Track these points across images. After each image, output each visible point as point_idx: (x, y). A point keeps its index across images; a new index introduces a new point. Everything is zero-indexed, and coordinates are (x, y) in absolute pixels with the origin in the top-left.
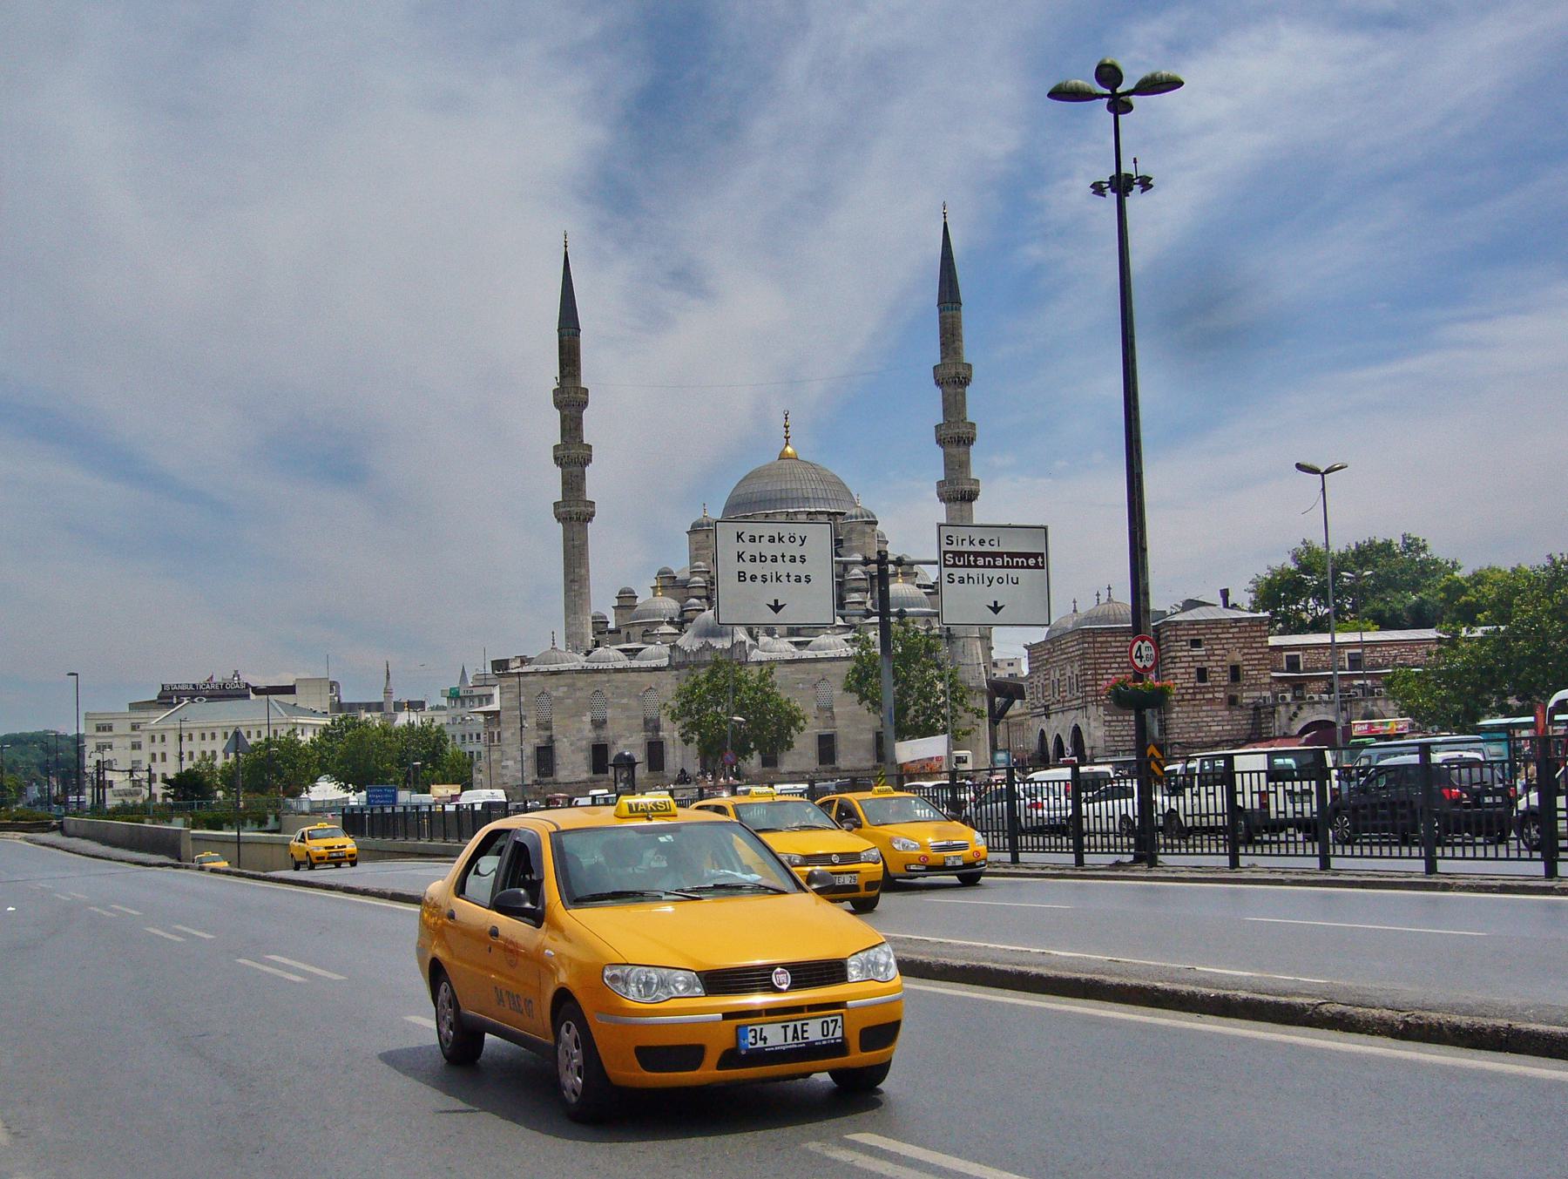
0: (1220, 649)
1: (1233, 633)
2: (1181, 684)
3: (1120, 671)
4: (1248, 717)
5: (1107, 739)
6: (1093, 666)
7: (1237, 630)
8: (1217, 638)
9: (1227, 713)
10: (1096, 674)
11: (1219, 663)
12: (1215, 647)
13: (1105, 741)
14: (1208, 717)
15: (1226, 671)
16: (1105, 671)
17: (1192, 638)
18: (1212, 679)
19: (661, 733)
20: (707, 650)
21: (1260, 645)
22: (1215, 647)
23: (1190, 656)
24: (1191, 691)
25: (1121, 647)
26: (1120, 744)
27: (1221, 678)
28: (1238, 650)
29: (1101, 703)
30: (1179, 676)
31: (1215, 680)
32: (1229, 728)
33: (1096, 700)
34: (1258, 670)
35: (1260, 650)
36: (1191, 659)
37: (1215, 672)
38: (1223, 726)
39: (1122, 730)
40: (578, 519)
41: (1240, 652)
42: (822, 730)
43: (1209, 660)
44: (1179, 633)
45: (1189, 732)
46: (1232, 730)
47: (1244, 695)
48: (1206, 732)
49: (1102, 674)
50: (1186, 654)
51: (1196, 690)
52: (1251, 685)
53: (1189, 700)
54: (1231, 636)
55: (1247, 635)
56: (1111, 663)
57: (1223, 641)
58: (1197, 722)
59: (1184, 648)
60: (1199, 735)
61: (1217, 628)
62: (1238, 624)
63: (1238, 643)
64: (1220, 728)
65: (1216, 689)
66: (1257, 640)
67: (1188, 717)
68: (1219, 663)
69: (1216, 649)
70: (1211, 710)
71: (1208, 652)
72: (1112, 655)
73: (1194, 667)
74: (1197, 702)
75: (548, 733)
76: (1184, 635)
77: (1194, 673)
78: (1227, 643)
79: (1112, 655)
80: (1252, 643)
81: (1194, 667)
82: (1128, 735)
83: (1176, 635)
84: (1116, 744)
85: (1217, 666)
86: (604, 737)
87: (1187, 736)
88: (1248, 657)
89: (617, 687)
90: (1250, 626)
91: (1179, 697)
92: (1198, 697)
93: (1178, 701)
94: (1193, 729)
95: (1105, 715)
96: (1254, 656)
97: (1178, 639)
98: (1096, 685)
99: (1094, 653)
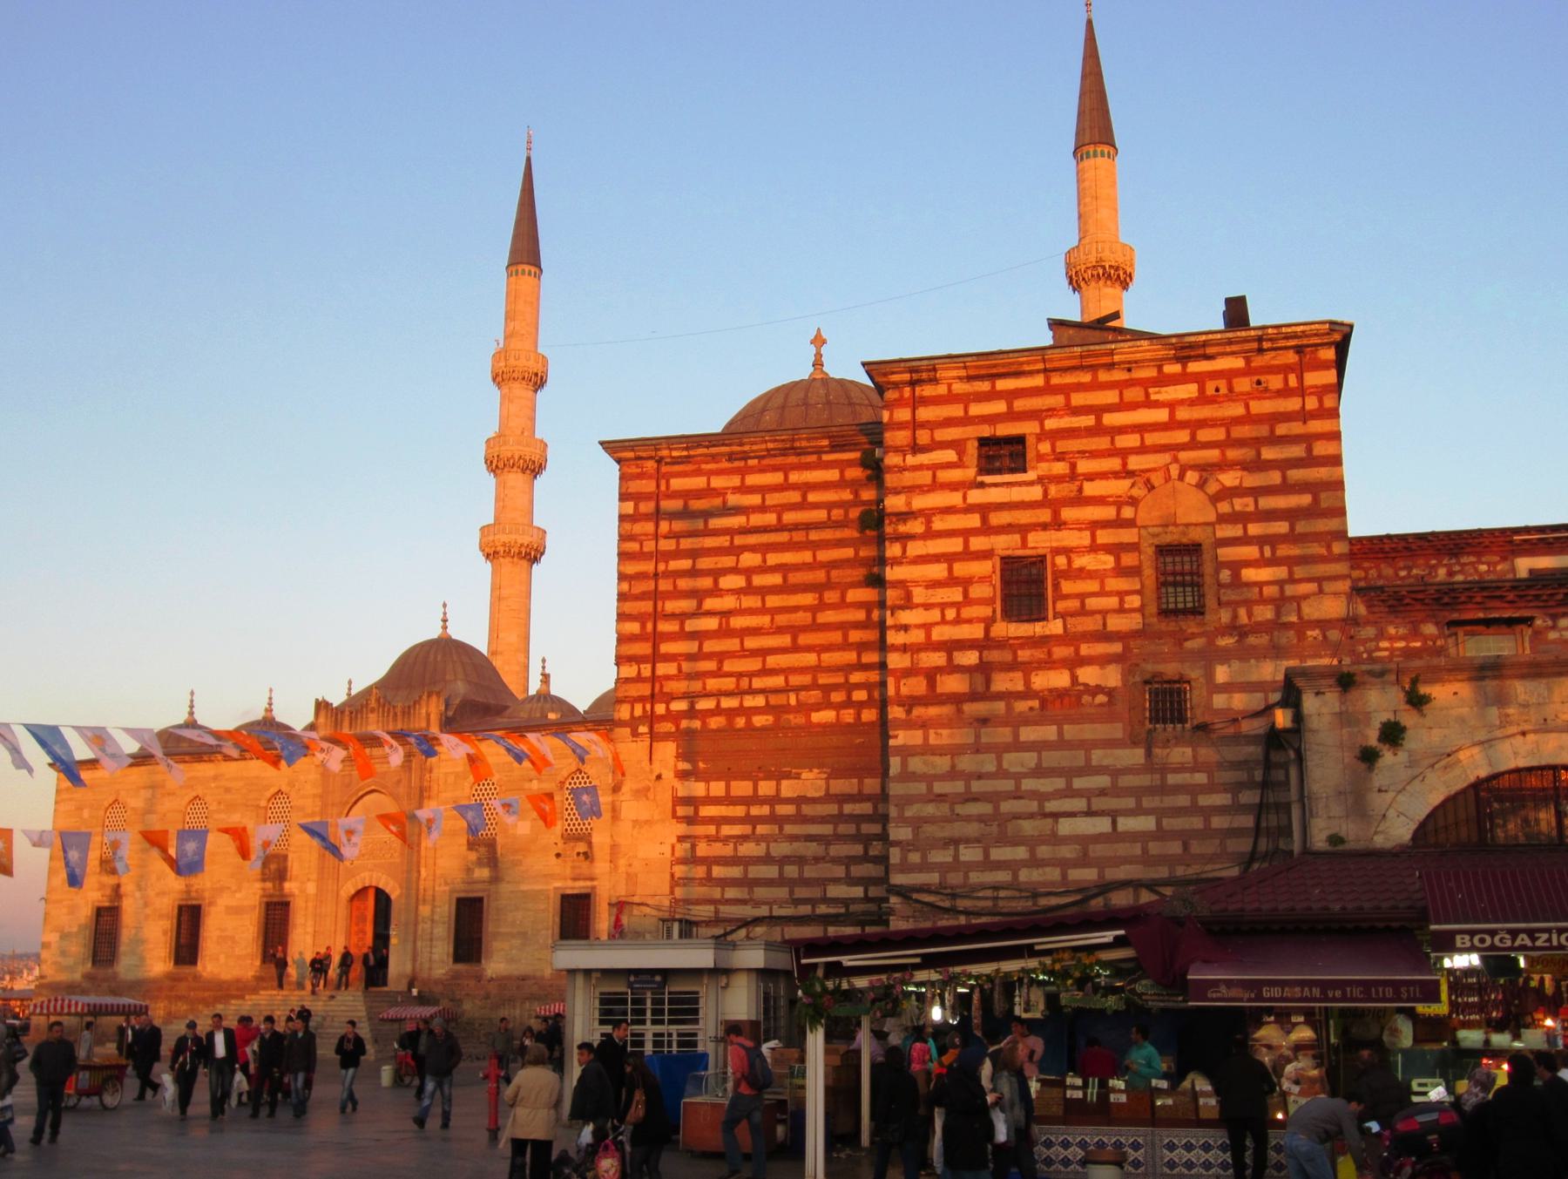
0: (1116, 475)
1: (1172, 405)
2: (927, 627)
3: (751, 602)
4: (1242, 776)
5: (680, 871)
6: (649, 586)
7: (1189, 390)
8: (1097, 430)
9: (1136, 756)
10: (656, 616)
11: (1104, 537)
12: (1084, 466)
13: (675, 882)
14: (1039, 772)
15: (1134, 572)
16: (686, 605)
17: (986, 431)
18: (1073, 604)
19: (287, 885)
20: (372, 711)
21: (1297, 451)
22: (1084, 466)
23: (969, 509)
24: (970, 658)
25: (763, 509)
26: (731, 893)
27: (1113, 602)
28: (1192, 477)
29: (668, 727)
30: (919, 595)
31: (1083, 612)
32: (1147, 823)
33: (652, 719)
34: (1290, 562)
35: (1295, 475)
36: (974, 521)
37: (1083, 574)
38: (1114, 815)
39: (744, 838)
40: (507, 553)
41: (1201, 485)
42: (570, 883)
43: (1058, 524)
44: (924, 414)
45: (955, 842)
46: (1160, 834)
47: (1222, 674)
48: (1032, 843)
49: (682, 617)
50: (955, 499)
51: (994, 656)
52: (1258, 628)
53: (956, 699)
54: (1162, 415)
55: (1237, 410)
56: (717, 574)
57: (1131, 441)
58: (994, 798)
59: (945, 476)
60: (998, 854)
61: (1096, 386)
62: (1194, 367)
63: (1193, 445)
64: (1102, 825)
65: (1085, 650)
66: (1281, 430)
67: (953, 774)
68: (1104, 537)
69: (1091, 477)
70: (1061, 744)
71: (1053, 491)
72: (723, 541)
73: (986, 555)
74: (1000, 706)
75: (110, 880)
76: (949, 422)
77: (983, 579)
78: (1143, 450)
79: (723, 541)
80: (1257, 442)
81: (986, 555)
82: (767, 859)
83: (915, 425)
84: (716, 893)
85: (1094, 548)
86: (197, 891)
87: (941, 856)
88: (1240, 504)
89: (228, 790)
90: (1247, 372)
91: (916, 686)
92: (1001, 683)
93: (910, 703)
94: (972, 829)
95: (683, 775)
96: (1267, 503)
97: (923, 437)
98: (655, 658)
99: (656, 537)
